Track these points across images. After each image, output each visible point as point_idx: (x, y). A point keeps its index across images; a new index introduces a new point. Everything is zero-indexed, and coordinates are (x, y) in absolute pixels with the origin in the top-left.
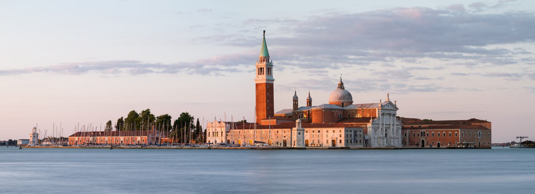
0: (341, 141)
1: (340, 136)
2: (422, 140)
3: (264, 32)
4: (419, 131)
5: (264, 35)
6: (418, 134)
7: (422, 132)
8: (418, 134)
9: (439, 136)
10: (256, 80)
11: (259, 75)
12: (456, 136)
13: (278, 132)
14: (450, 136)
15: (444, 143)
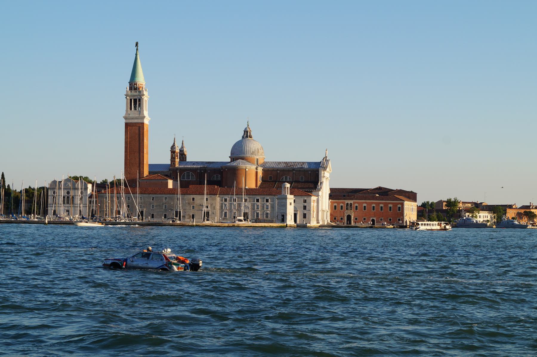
0: (305, 216)
1: (305, 208)
2: (347, 214)
3: (137, 44)
4: (343, 203)
5: (137, 49)
6: (342, 206)
7: (347, 204)
8: (342, 206)
9: (374, 209)
10: (125, 118)
11: (131, 109)
12: (399, 210)
13: (193, 199)
14: (390, 210)
15: (381, 220)
